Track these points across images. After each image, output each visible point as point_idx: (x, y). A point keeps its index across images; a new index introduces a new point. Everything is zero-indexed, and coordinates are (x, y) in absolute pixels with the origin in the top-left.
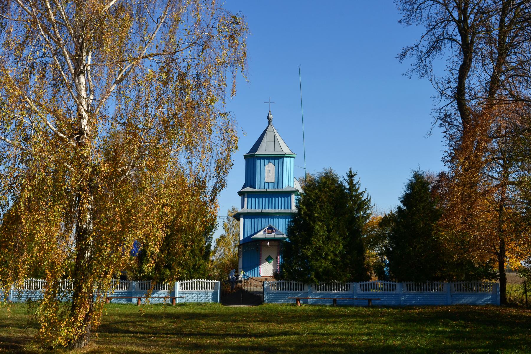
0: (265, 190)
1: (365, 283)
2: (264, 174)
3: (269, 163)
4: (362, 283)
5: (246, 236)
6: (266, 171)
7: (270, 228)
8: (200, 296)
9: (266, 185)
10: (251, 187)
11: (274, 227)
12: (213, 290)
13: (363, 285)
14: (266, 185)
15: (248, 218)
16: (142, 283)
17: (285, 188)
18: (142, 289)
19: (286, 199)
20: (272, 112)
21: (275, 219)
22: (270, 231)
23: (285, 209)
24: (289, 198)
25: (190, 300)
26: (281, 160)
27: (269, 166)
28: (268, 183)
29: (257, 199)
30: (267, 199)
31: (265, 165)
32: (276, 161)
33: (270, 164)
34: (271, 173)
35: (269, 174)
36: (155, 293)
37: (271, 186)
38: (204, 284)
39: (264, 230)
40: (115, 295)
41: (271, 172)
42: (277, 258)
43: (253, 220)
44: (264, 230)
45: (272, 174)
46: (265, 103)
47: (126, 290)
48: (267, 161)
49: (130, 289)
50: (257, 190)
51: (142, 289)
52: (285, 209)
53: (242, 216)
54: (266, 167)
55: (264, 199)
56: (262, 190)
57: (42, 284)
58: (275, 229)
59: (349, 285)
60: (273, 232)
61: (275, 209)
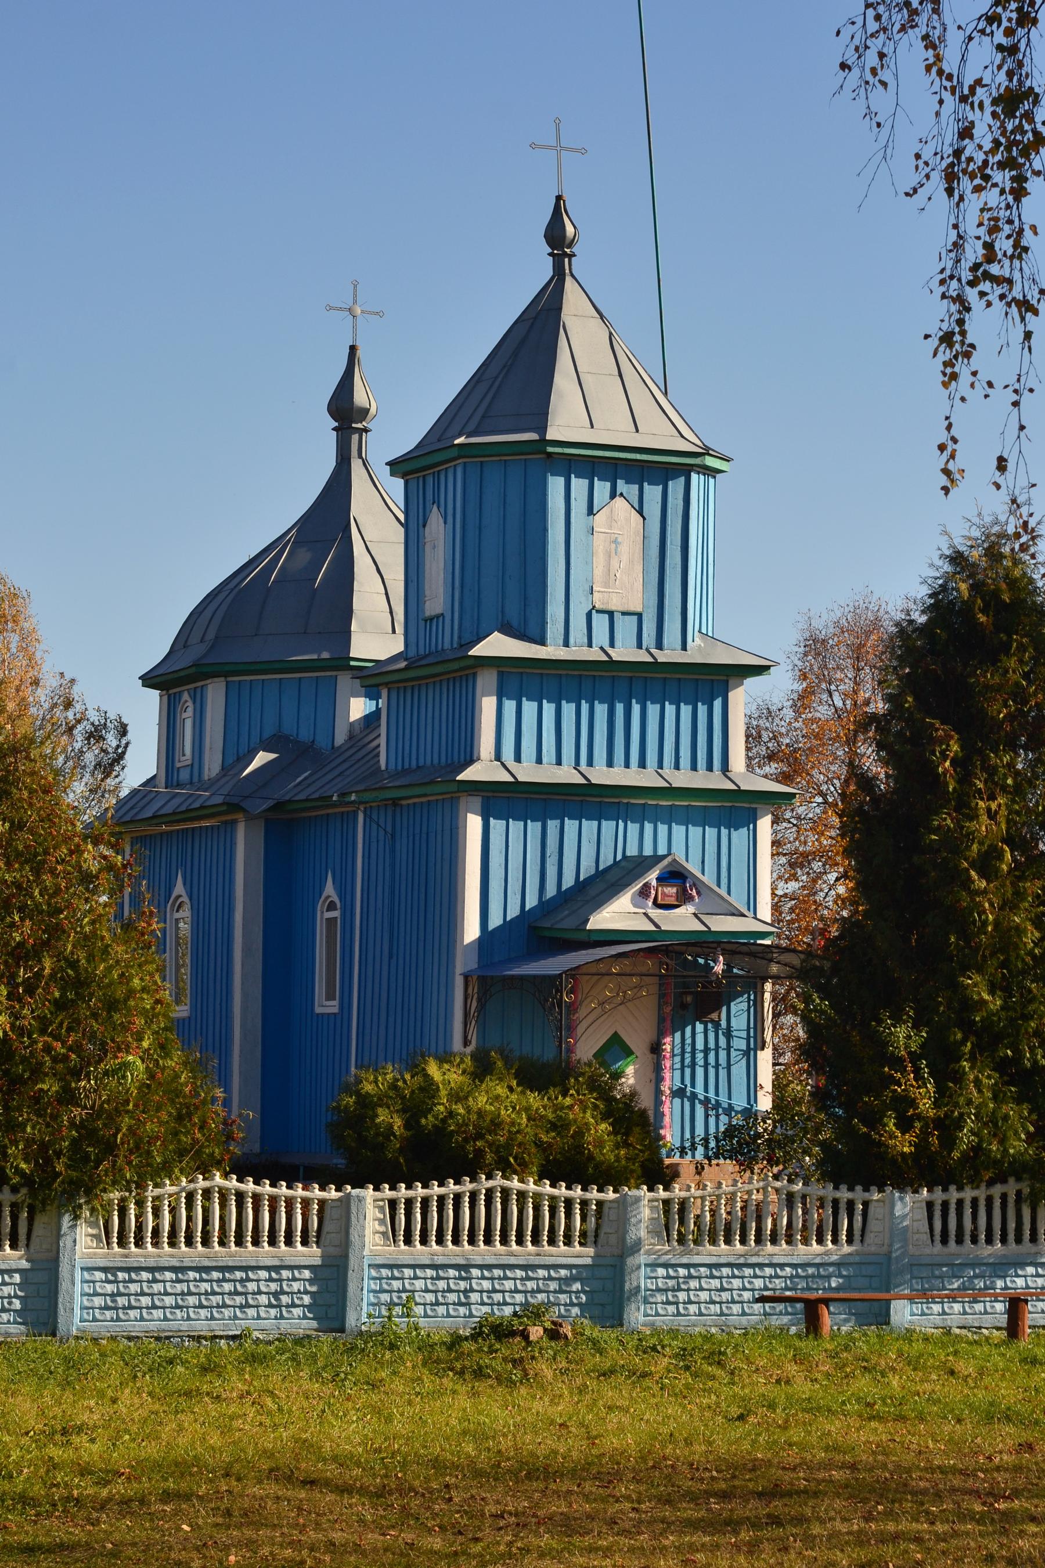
0: (594, 654)
1: (419, 1191)
2: (589, 563)
3: (613, 495)
4: (403, 1192)
5: (495, 921)
6: (599, 542)
7: (676, 876)
8: (252, 1286)
9: (601, 623)
10: (509, 630)
11: (693, 867)
12: (314, 1249)
13: (409, 1203)
14: (601, 623)
15: (505, 816)
16: (945, 1205)
17: (698, 652)
18: (944, 1241)
19: (702, 709)
20: (571, 204)
21: (648, 827)
22: (672, 890)
23: (539, 761)
24: (718, 704)
25: (158, 1314)
26: (676, 487)
27: (611, 519)
28: (611, 614)
29: (686, 710)
30: (686, 710)
31: (591, 512)
32: (653, 493)
33: (619, 501)
34: (625, 558)
35: (615, 563)
36: (1023, 1265)
37: (626, 628)
38: (537, 1209)
39: (638, 886)
40: (779, 1283)
41: (624, 549)
42: (656, 1049)
43: (534, 828)
44: (638, 886)
45: (631, 561)
46: (533, 146)
47: (846, 1249)
48: (602, 488)
49: (870, 1237)
50: (552, 651)
51: (944, 1241)
52: (539, 761)
53: (477, 802)
54: (600, 520)
55: (585, 706)
56: (578, 652)
57: (569, 1214)
58: (697, 884)
59: (866, 1204)
60: (685, 898)
61: (642, 764)
